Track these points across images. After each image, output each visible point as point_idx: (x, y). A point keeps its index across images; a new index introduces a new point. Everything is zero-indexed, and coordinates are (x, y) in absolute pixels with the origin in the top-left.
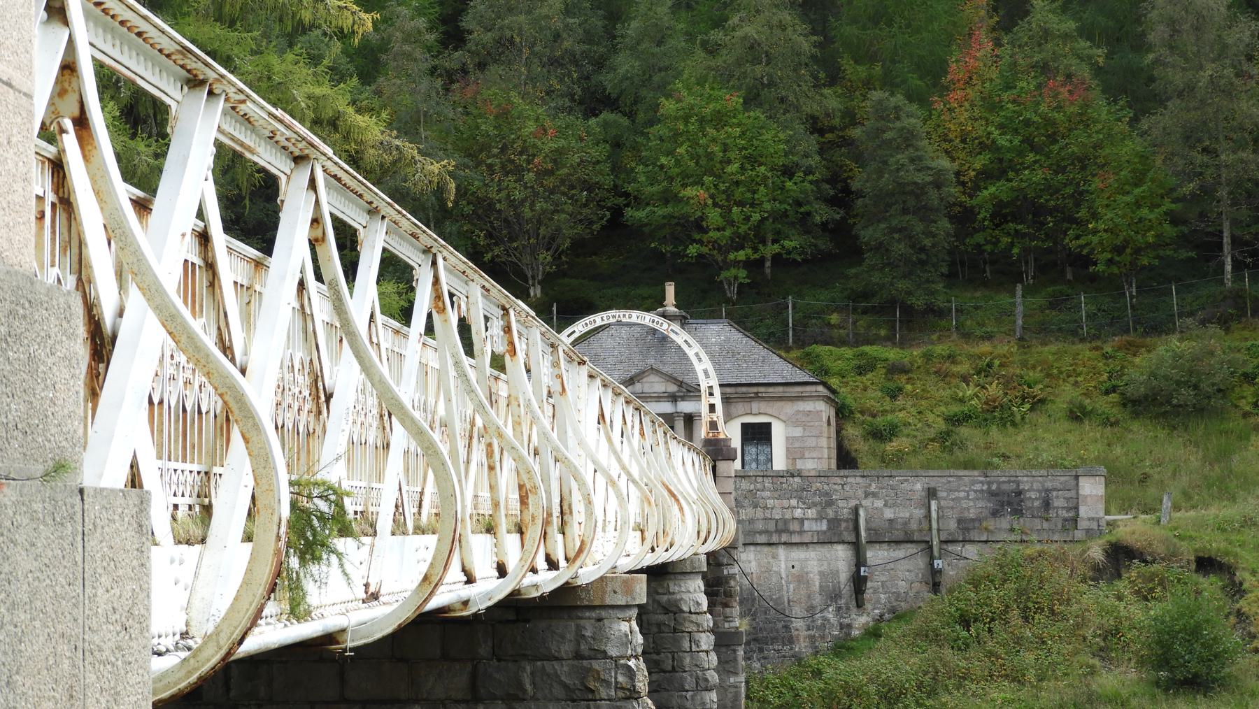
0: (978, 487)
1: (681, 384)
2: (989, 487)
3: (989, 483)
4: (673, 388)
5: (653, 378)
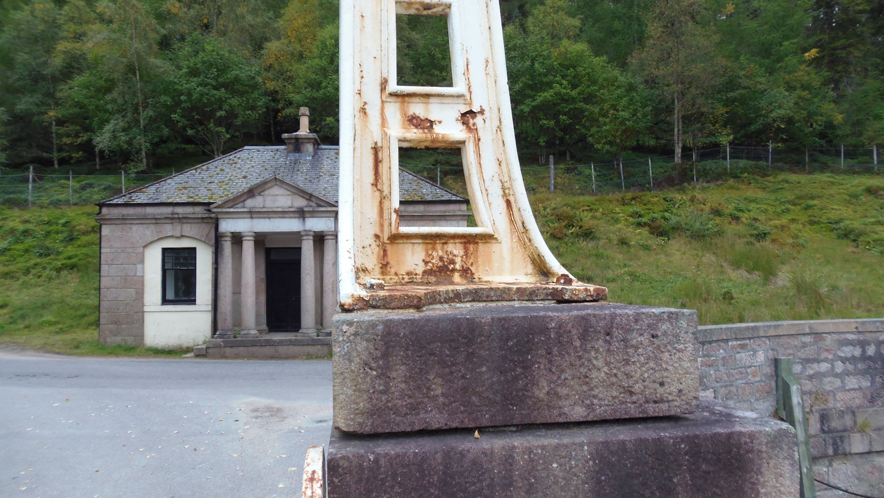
0: (848, 351)
1: (309, 197)
2: (864, 351)
3: (863, 344)
4: (300, 202)
5: (276, 190)
